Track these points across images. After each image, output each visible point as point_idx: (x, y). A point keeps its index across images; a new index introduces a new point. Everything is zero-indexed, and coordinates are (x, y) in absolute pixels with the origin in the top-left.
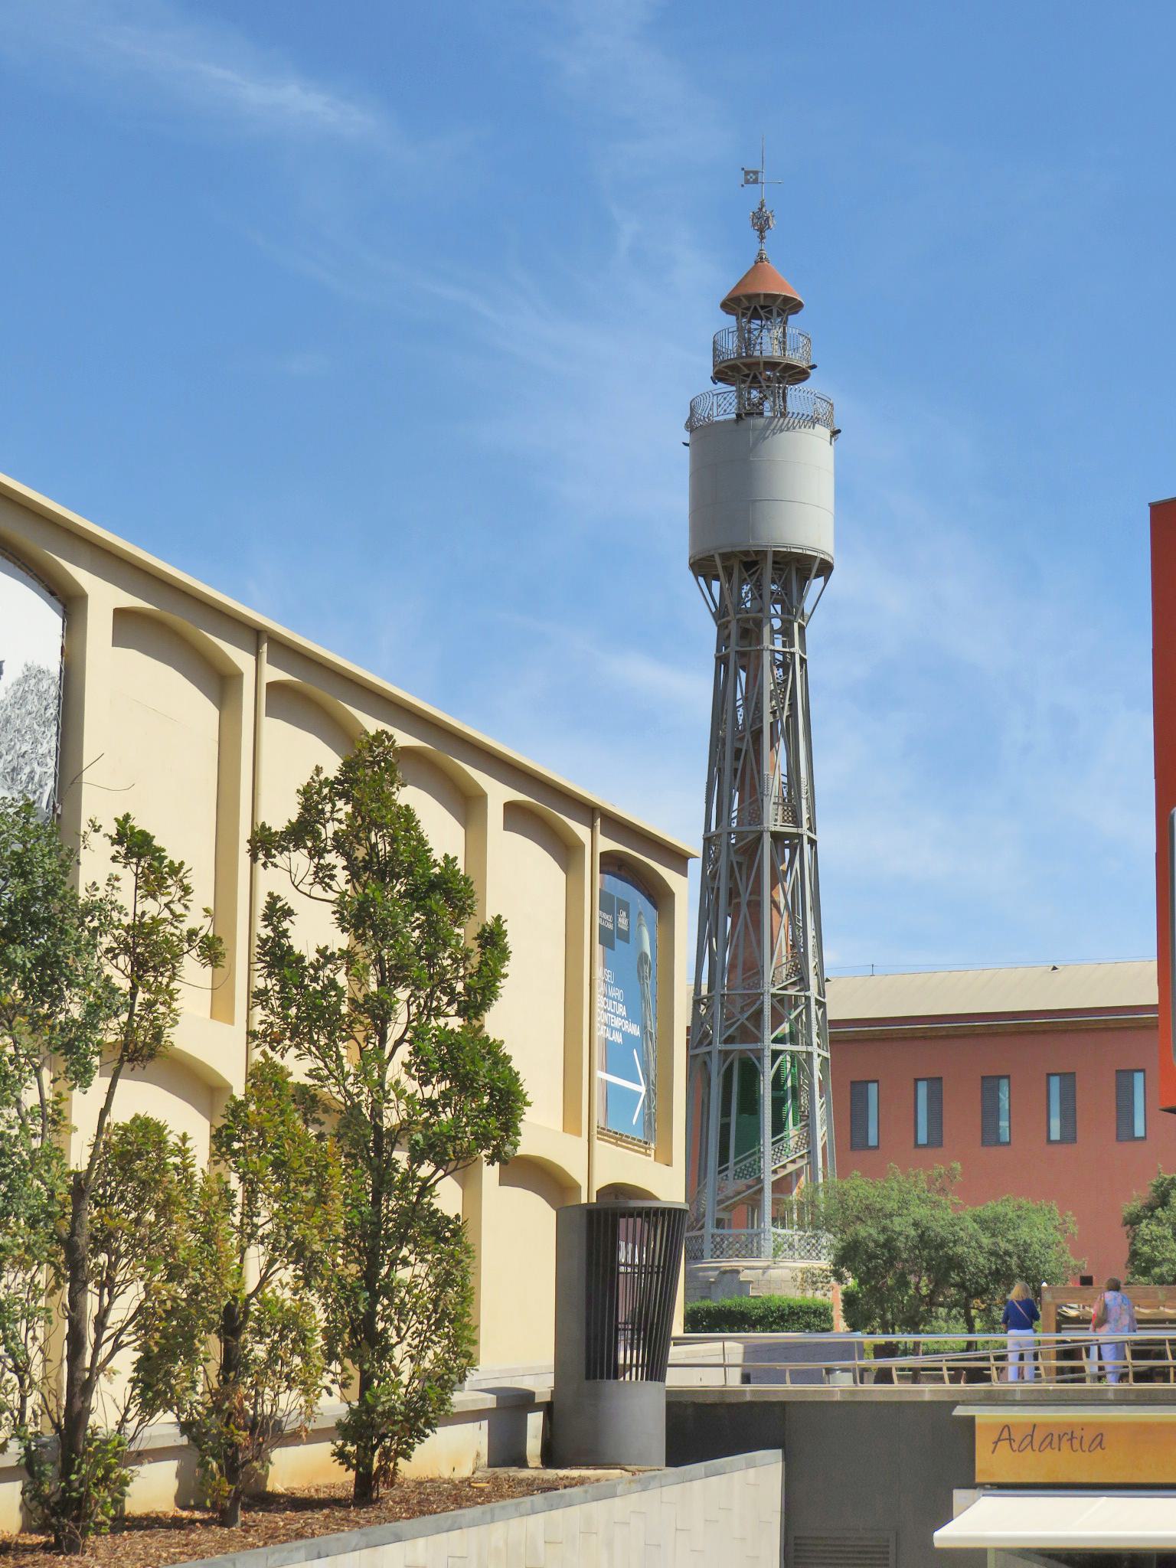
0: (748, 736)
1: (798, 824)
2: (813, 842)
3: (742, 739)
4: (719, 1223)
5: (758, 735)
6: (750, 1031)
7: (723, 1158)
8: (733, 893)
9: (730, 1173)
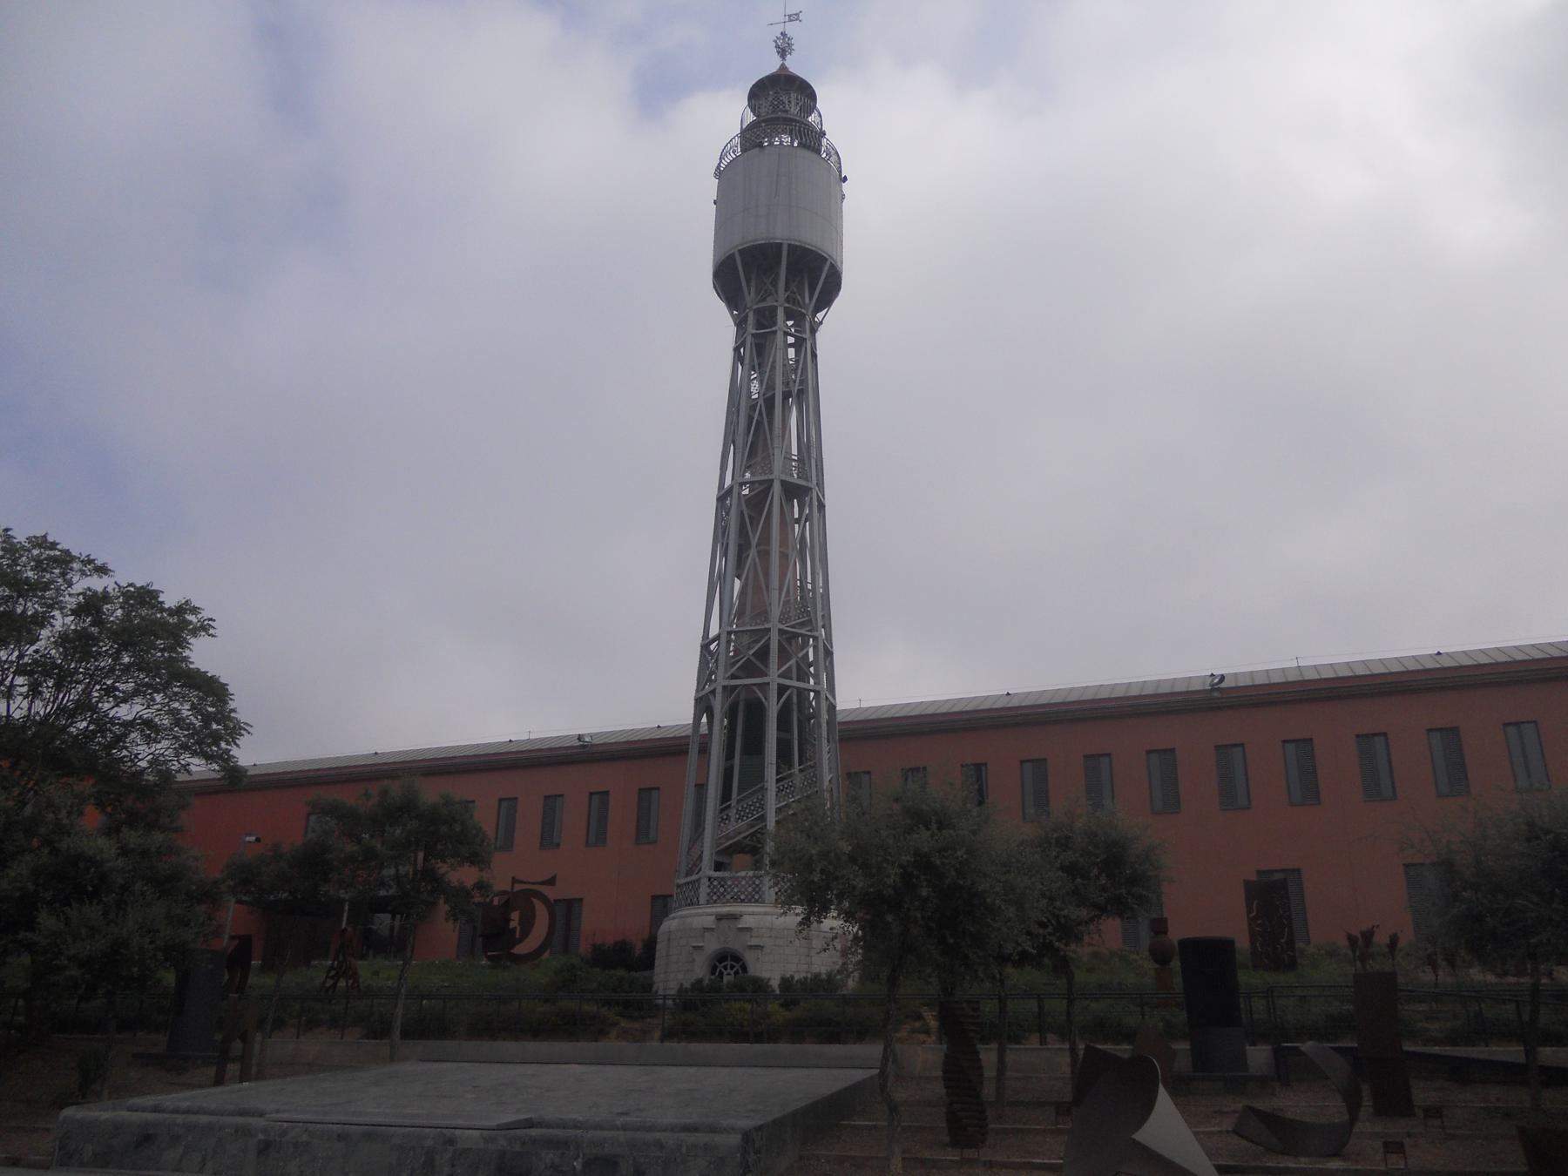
0: (761, 402)
1: (807, 479)
2: (822, 506)
3: (753, 408)
4: (718, 866)
5: (770, 402)
6: (754, 665)
7: (726, 796)
8: (743, 549)
9: (732, 812)
